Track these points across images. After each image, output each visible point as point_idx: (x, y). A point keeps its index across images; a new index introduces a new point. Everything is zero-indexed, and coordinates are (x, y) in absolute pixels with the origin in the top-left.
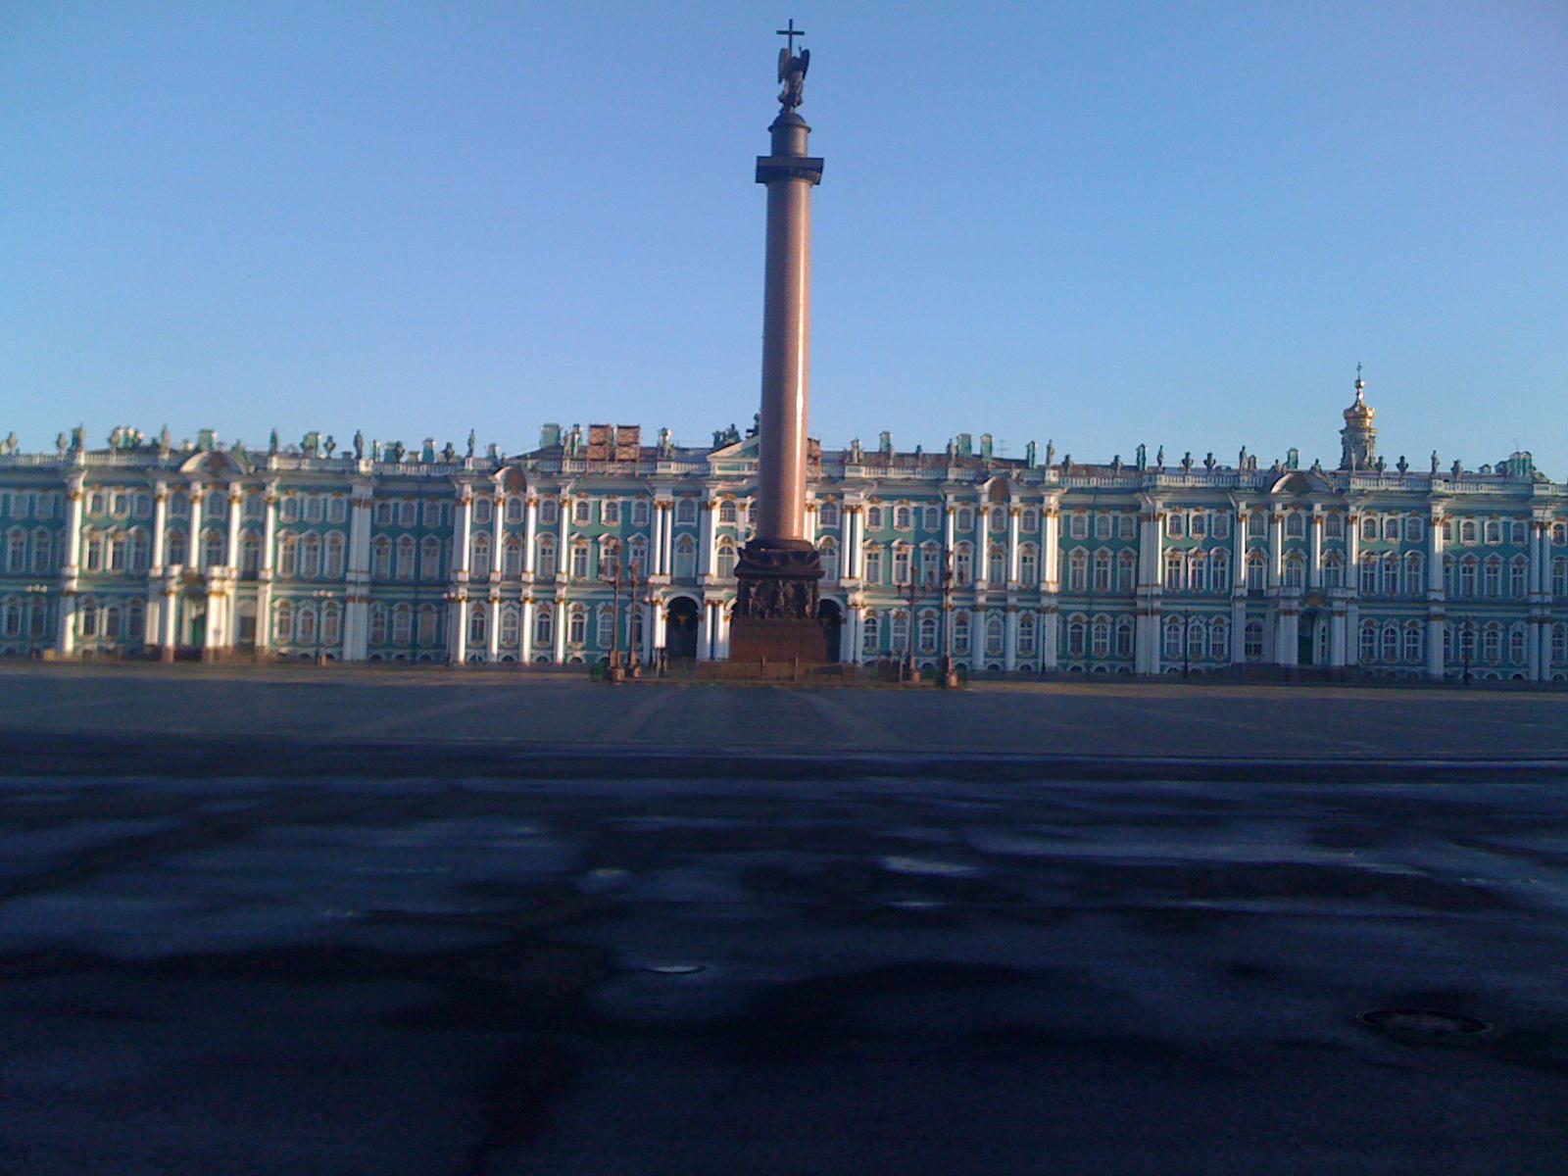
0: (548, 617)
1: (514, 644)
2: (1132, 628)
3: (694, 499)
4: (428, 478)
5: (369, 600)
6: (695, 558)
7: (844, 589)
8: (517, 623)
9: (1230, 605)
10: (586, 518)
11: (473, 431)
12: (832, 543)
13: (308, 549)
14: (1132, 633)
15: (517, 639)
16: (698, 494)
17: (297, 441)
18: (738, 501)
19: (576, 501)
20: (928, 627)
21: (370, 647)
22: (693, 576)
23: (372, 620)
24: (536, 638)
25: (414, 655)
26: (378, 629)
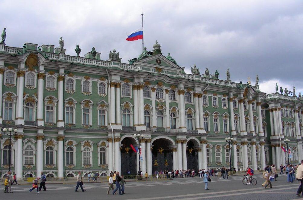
0: (52, 149)
2: (268, 152)
3: (130, 84)
7: (200, 134)
8: (34, 152)
9: (297, 142)
11: (5, 29)
12: (191, 111)
14: (268, 154)
15: (34, 163)
16: (132, 81)
18: (151, 86)
19: (67, 78)
20: (227, 152)
22: (132, 125)
24: (45, 163)
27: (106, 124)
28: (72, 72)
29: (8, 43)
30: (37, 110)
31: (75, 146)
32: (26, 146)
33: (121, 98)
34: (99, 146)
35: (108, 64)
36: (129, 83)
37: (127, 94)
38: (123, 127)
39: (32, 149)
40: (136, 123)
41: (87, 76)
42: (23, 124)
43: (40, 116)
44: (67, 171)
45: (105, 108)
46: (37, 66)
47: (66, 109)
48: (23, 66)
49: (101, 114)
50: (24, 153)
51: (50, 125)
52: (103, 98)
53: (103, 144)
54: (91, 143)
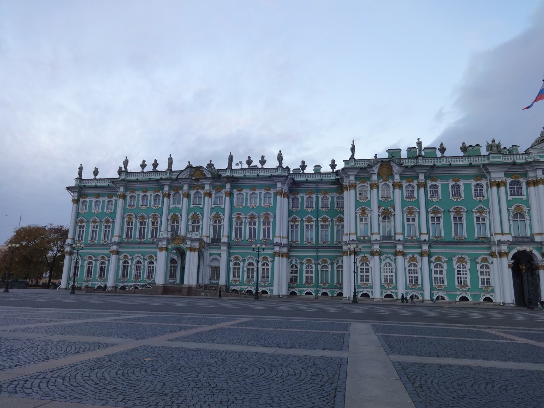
1: (392, 285)
3: (523, 180)
4: (322, 181)
5: (288, 257)
6: (528, 223)
8: (394, 270)
10: (437, 196)
11: (353, 142)
13: (250, 223)
15: (394, 282)
16: (525, 175)
17: (244, 160)
19: (429, 183)
21: (289, 286)
22: (529, 235)
23: (290, 270)
24: (408, 283)
25: (317, 292)
26: (294, 275)
27: (489, 235)
28: (434, 176)
29: (357, 157)
30: (395, 223)
31: (445, 262)
32: (383, 263)
33: (508, 201)
34: (478, 263)
35: (486, 159)
36: (520, 179)
37: (518, 194)
38: (513, 237)
39: (391, 266)
40: (536, 230)
41: (456, 179)
42: (378, 239)
43: (399, 229)
44: (435, 292)
45: (484, 215)
46: (392, 175)
47: (430, 219)
48: (375, 178)
49: (479, 222)
50: (382, 270)
51: (412, 239)
52: (480, 202)
53: (485, 260)
54: (467, 259)
